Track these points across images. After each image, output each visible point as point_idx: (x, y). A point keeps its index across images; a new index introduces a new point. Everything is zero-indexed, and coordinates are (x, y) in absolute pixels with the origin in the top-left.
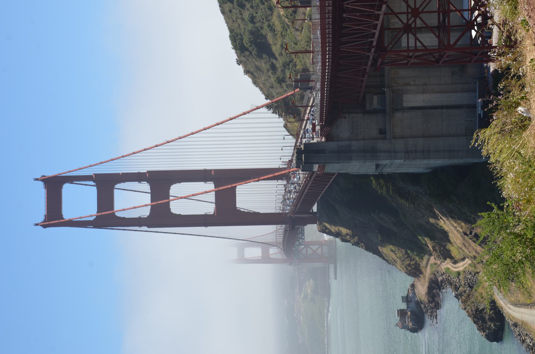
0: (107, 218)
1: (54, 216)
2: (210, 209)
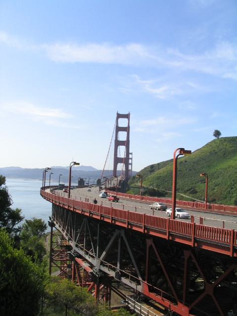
0: (118, 129)
1: (119, 116)
2: (118, 156)
